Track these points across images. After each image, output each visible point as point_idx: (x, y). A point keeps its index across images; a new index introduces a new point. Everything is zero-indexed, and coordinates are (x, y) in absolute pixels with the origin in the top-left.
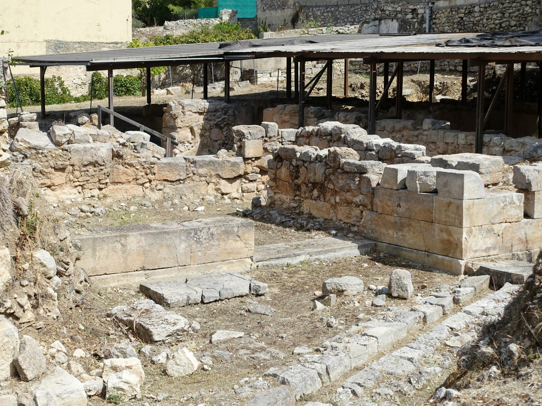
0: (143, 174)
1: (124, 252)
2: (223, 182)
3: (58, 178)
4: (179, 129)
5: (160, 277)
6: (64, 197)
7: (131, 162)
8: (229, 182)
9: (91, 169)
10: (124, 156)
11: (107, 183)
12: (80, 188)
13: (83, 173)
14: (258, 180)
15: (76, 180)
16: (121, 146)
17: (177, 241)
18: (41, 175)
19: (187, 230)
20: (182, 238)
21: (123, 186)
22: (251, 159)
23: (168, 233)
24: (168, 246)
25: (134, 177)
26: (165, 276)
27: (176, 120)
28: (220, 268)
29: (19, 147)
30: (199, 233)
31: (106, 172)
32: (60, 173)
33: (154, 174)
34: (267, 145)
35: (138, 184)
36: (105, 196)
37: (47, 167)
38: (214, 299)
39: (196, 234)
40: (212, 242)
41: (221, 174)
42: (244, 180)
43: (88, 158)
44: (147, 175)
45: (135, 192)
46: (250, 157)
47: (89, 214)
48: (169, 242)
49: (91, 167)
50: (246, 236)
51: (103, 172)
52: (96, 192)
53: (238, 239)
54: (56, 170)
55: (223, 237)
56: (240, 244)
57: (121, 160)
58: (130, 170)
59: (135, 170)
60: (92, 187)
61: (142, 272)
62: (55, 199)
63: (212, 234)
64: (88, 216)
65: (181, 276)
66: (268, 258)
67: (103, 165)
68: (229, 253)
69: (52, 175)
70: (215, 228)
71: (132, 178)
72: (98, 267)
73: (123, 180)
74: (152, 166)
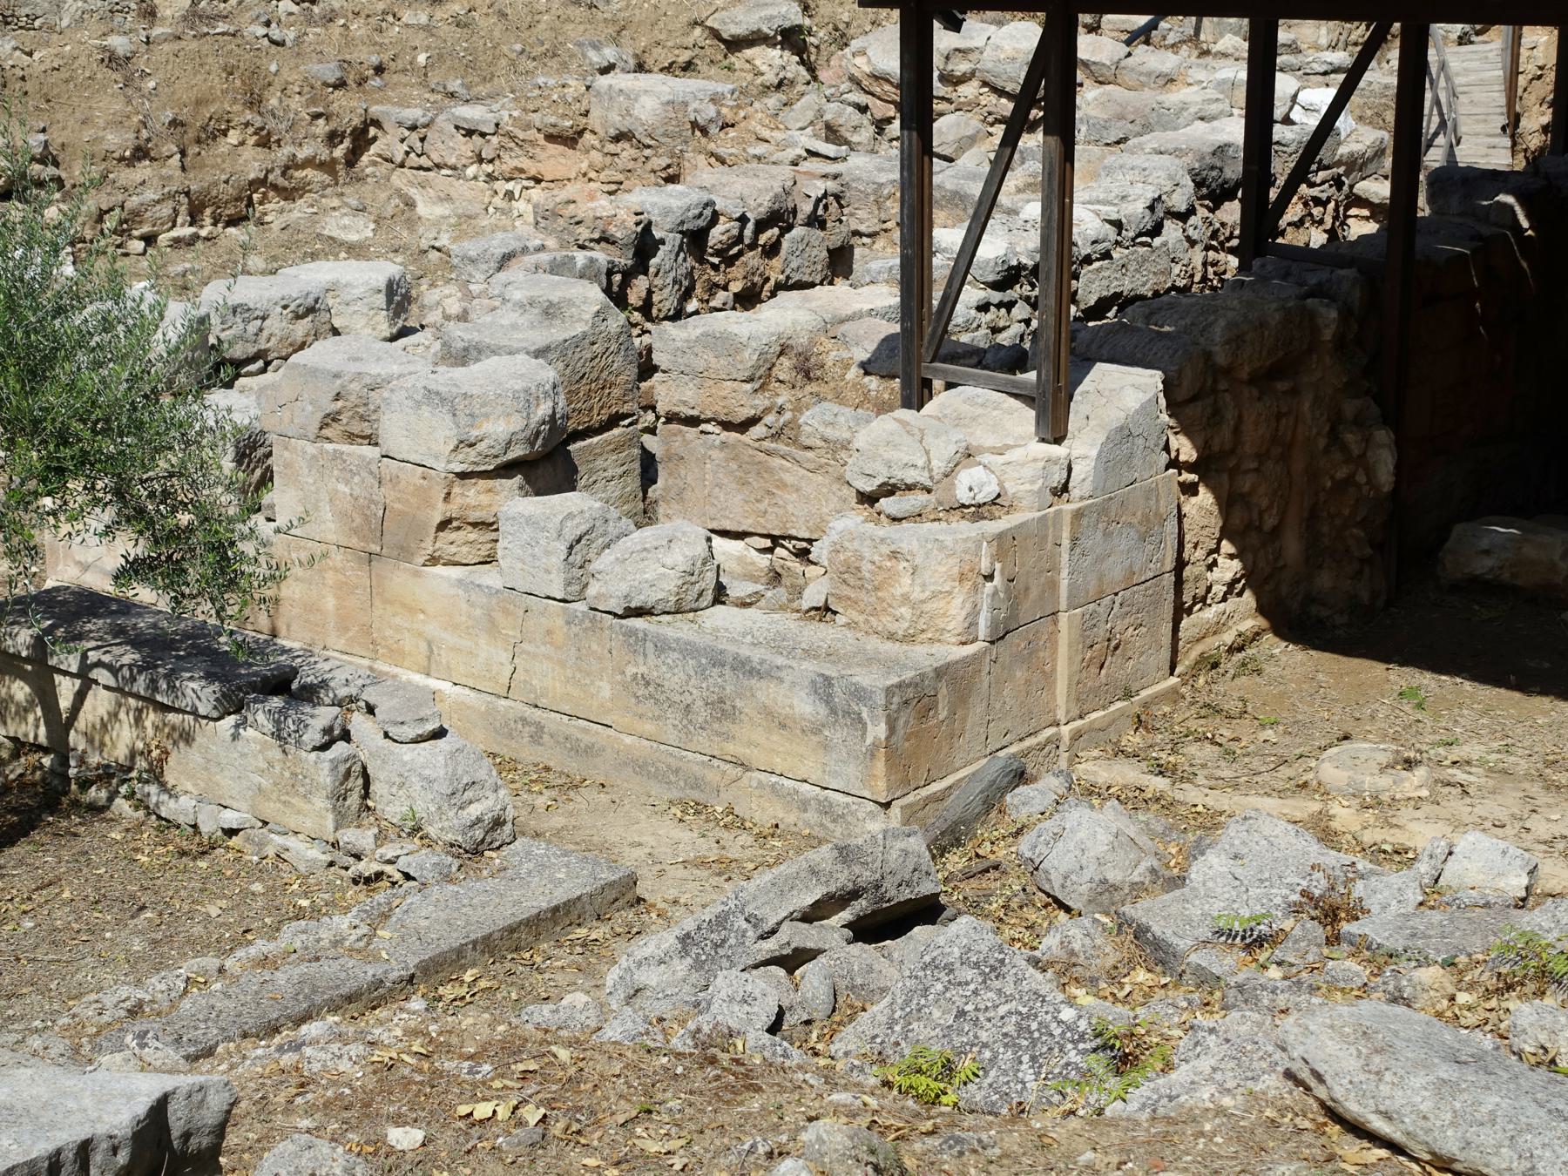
3: (554, 160)
7: (721, 151)
9: (626, 151)
10: (713, 130)
13: (608, 159)
15: (593, 175)
18: (512, 145)
29: (853, 71)
31: (656, 168)
32: (561, 148)
37: (527, 127)
43: (617, 122)
49: (626, 145)
51: (649, 166)
54: (550, 138)
57: (704, 140)
67: (649, 147)
69: (538, 150)
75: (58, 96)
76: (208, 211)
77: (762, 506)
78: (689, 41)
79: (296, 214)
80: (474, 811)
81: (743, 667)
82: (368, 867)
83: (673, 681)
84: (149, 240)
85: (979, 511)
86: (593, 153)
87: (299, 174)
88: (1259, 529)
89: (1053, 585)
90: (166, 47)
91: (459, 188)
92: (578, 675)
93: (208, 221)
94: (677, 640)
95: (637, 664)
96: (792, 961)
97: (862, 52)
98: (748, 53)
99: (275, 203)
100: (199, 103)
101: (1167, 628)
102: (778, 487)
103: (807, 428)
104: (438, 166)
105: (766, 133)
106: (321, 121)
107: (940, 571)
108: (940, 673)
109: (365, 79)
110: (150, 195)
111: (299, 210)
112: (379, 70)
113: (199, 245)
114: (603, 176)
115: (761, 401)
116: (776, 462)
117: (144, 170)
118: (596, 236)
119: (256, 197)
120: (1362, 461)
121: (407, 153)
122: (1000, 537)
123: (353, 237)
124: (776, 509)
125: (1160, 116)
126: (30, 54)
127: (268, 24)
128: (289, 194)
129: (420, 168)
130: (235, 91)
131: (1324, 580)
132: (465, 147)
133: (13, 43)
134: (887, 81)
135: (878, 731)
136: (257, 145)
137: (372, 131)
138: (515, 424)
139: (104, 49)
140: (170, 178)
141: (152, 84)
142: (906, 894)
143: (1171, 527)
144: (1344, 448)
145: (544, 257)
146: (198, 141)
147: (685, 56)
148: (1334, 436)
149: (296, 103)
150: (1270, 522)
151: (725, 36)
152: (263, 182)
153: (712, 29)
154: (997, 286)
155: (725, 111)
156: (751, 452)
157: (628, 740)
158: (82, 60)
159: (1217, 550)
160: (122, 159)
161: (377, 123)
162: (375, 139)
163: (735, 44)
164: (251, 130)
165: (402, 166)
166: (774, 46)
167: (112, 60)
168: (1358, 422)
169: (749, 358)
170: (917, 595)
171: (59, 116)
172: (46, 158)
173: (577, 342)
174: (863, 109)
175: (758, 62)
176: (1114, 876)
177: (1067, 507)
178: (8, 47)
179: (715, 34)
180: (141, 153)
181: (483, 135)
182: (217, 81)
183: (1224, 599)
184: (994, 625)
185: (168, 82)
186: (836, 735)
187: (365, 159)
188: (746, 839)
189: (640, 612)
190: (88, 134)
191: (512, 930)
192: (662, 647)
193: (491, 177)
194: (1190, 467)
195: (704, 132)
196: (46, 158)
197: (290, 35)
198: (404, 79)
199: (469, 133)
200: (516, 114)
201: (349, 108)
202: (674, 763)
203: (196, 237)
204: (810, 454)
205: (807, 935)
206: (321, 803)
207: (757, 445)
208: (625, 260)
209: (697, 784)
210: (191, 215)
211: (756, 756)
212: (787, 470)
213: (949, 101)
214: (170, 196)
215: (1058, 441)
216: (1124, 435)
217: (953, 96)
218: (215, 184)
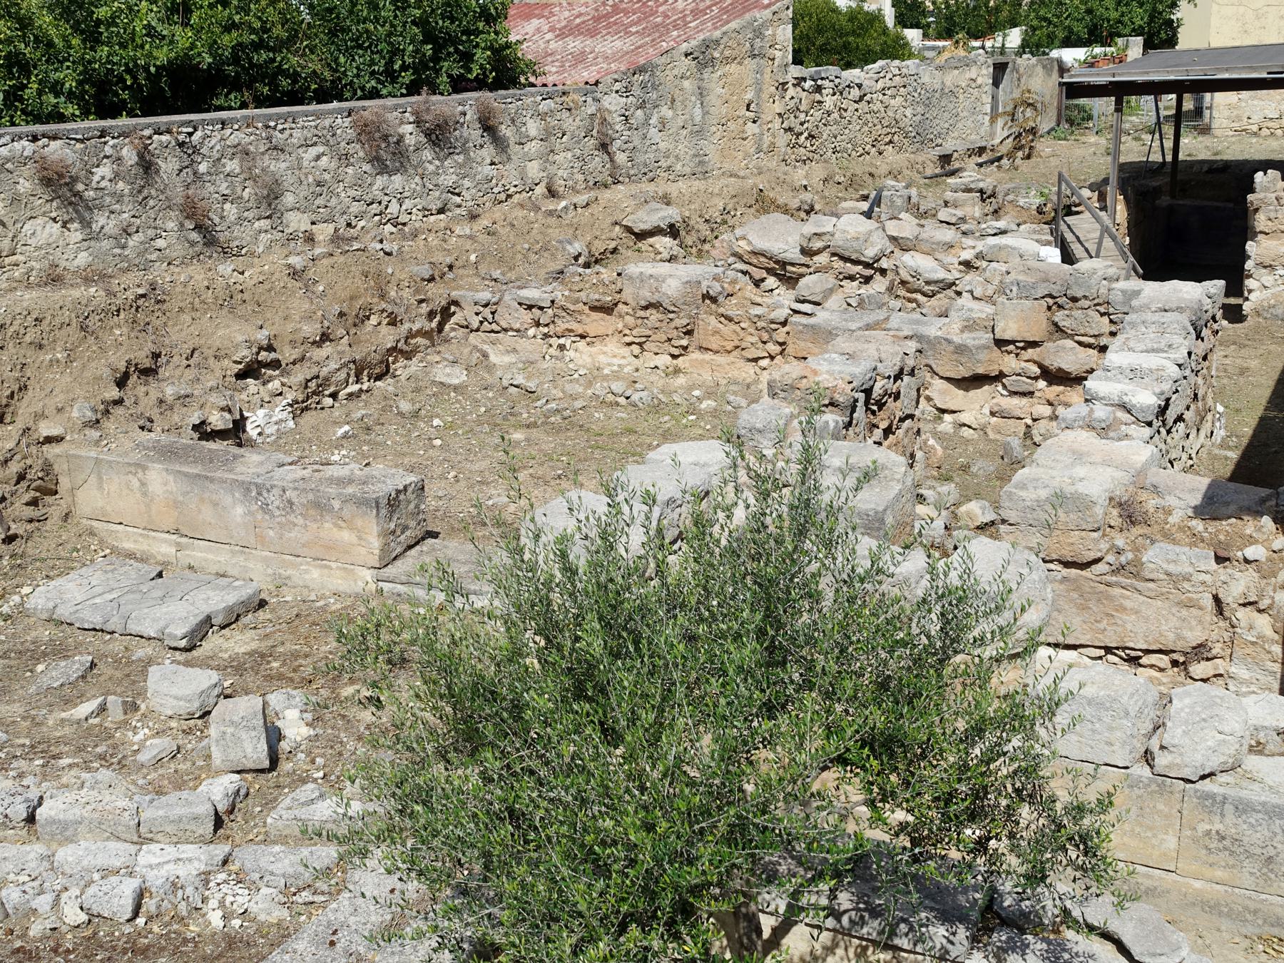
0: (754, 339)
1: (145, 494)
2: (938, 384)
3: (596, 323)
4: (1260, 237)
5: (200, 554)
6: (603, 359)
7: (729, 313)
8: (959, 387)
9: (654, 315)
10: (721, 299)
11: (685, 348)
12: (636, 349)
13: (639, 321)
14: (1037, 394)
15: (627, 332)
16: (962, 267)
17: (228, 500)
19: (243, 482)
20: (237, 495)
21: (714, 357)
22: (1013, 342)
23: (212, 480)
24: (216, 505)
25: (737, 343)
26: (210, 556)
27: (1257, 216)
28: (306, 572)
29: (738, 249)
30: (265, 495)
32: (601, 315)
33: (781, 344)
34: (1059, 316)
35: (743, 357)
36: (677, 371)
37: (577, 301)
38: (91, 626)
39: (259, 494)
40: (292, 518)
41: (934, 366)
42: (1000, 388)
43: (647, 295)
44: (765, 343)
45: (736, 373)
46: (1007, 337)
47: (622, 400)
48: (214, 497)
49: (654, 311)
50: (359, 522)
51: (673, 325)
52: (664, 360)
53: (343, 524)
54: (593, 309)
55: (312, 512)
56: (346, 536)
57: (713, 306)
58: (728, 329)
59: (738, 329)
60: (656, 350)
61: (174, 537)
62: (589, 360)
63: (291, 503)
64: (617, 404)
65: (234, 565)
66: (404, 579)
68: (328, 548)
69: (584, 317)
70: (296, 493)
71: (733, 344)
72: (109, 508)
73: (714, 347)
74: (773, 326)
75: (265, 301)
76: (365, 372)
77: (1101, 626)
78: (614, 235)
79: (413, 368)
86: (628, 317)
87: (413, 341)
90: (325, 262)
91: (522, 343)
92: (1138, 829)
93: (366, 379)
94: (1264, 804)
95: (1211, 822)
97: (744, 238)
98: (651, 240)
99: (402, 362)
100: (352, 298)
102: (1117, 610)
103: (1151, 565)
104: (506, 330)
105: (759, 300)
106: (424, 305)
109: (444, 274)
110: (333, 365)
111: (414, 366)
112: (451, 267)
113: (363, 397)
114: (634, 332)
116: (1117, 591)
117: (327, 349)
118: (827, 402)
119: (391, 359)
121: (481, 322)
123: (456, 381)
124: (1114, 628)
125: (1076, 278)
126: (242, 273)
127: (381, 241)
128: (408, 355)
129: (492, 331)
130: (372, 288)
132: (526, 317)
133: (232, 267)
134: (763, 255)
136: (389, 324)
137: (453, 308)
139: (289, 266)
140: (343, 352)
141: (321, 288)
146: (355, 325)
147: (612, 245)
149: (406, 293)
151: (636, 230)
152: (394, 349)
153: (626, 227)
155: (726, 286)
156: (1092, 584)
157: (1198, 884)
158: (277, 275)
160: (314, 343)
161: (456, 303)
162: (454, 313)
163: (642, 236)
164: (385, 314)
165: (477, 330)
166: (665, 235)
167: (295, 274)
171: (269, 315)
172: (270, 348)
174: (745, 273)
175: (657, 246)
178: (229, 270)
179: (629, 230)
180: (325, 337)
181: (541, 308)
182: (359, 282)
185: (330, 286)
187: (447, 327)
190: (290, 327)
193: (546, 336)
195: (714, 300)
198: (466, 272)
199: (530, 307)
200: (566, 293)
201: (438, 294)
202: (1252, 906)
203: (361, 390)
204: (1151, 585)
207: (1098, 579)
210: (357, 376)
212: (1128, 598)
213: (808, 266)
214: (345, 365)
217: (810, 263)
218: (369, 354)
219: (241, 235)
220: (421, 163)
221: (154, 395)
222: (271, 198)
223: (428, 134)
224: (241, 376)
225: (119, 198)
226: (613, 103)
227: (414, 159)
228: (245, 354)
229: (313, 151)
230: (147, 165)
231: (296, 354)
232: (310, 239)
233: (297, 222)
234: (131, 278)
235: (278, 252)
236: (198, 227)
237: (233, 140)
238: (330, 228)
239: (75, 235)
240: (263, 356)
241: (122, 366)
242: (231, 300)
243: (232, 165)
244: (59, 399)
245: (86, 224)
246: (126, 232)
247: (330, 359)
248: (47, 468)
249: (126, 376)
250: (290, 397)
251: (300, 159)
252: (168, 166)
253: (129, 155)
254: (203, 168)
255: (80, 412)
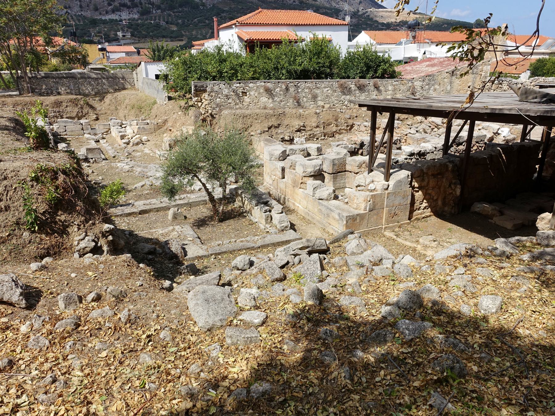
80: (283, 225)
81: (330, 209)
82: (268, 230)
83: (323, 210)
84: (317, 139)
85: (371, 191)
88: (433, 199)
89: (383, 204)
96: (295, 255)
99: (337, 135)
101: (408, 213)
107: (361, 199)
108: (357, 215)
110: (318, 132)
111: (341, 136)
112: (356, 117)
115: (359, 170)
117: (318, 129)
120: (454, 190)
122: (372, 195)
128: (340, 134)
131: (446, 209)
135: (345, 222)
138: (312, 170)
142: (319, 248)
143: (410, 197)
144: (451, 188)
145: (343, 146)
148: (450, 186)
149: (343, 121)
150: (435, 198)
154: (409, 156)
159: (423, 201)
167: (316, 113)
168: (455, 184)
169: (358, 163)
170: (357, 202)
173: (340, 159)
176: (355, 251)
177: (387, 192)
180: (317, 127)
182: (331, 117)
183: (424, 209)
184: (369, 209)
186: (340, 222)
188: (327, 235)
189: (321, 199)
191: (278, 243)
192: (322, 205)
194: (417, 188)
196: (304, 126)
197: (344, 111)
201: (350, 122)
203: (324, 139)
205: (299, 252)
206: (264, 220)
208: (358, 147)
209: (324, 226)
211: (331, 223)
215: (388, 181)
216: (400, 182)
219: (307, 104)
220: (355, 94)
221: (276, 131)
222: (315, 97)
223: (358, 88)
224: (296, 131)
225: (280, 95)
226: (418, 84)
227: (353, 93)
228: (297, 127)
229: (327, 89)
230: (287, 89)
231: (310, 129)
232: (323, 107)
233: (321, 103)
234: (279, 110)
235: (315, 108)
236: (298, 102)
237: (308, 85)
238: (329, 105)
239: (270, 101)
240: (302, 128)
241: (271, 125)
242: (300, 116)
243: (307, 90)
244: (256, 129)
245: (273, 99)
246: (281, 101)
247: (317, 131)
248: (251, 141)
249: (271, 127)
250: (305, 137)
251: (323, 91)
252: (292, 90)
253: (284, 87)
254: (299, 90)
255: (259, 132)
